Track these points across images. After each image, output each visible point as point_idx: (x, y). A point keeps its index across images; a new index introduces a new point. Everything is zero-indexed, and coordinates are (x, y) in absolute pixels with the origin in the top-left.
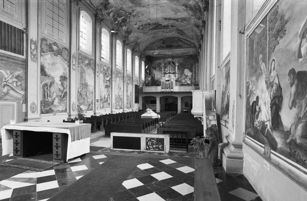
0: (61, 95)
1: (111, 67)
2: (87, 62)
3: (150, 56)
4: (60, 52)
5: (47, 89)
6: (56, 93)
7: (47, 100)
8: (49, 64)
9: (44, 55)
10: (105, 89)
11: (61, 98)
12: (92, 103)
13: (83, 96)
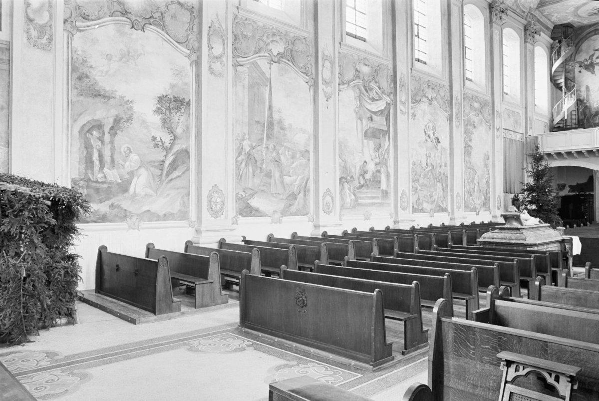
0: (163, 161)
1: (391, 66)
2: (278, 48)
3: (568, 26)
4: (157, 15)
5: (101, 139)
6: (139, 155)
7: (101, 175)
8: (109, 57)
9: (88, 26)
10: (365, 141)
11: (162, 170)
12: (306, 191)
13: (264, 166)
